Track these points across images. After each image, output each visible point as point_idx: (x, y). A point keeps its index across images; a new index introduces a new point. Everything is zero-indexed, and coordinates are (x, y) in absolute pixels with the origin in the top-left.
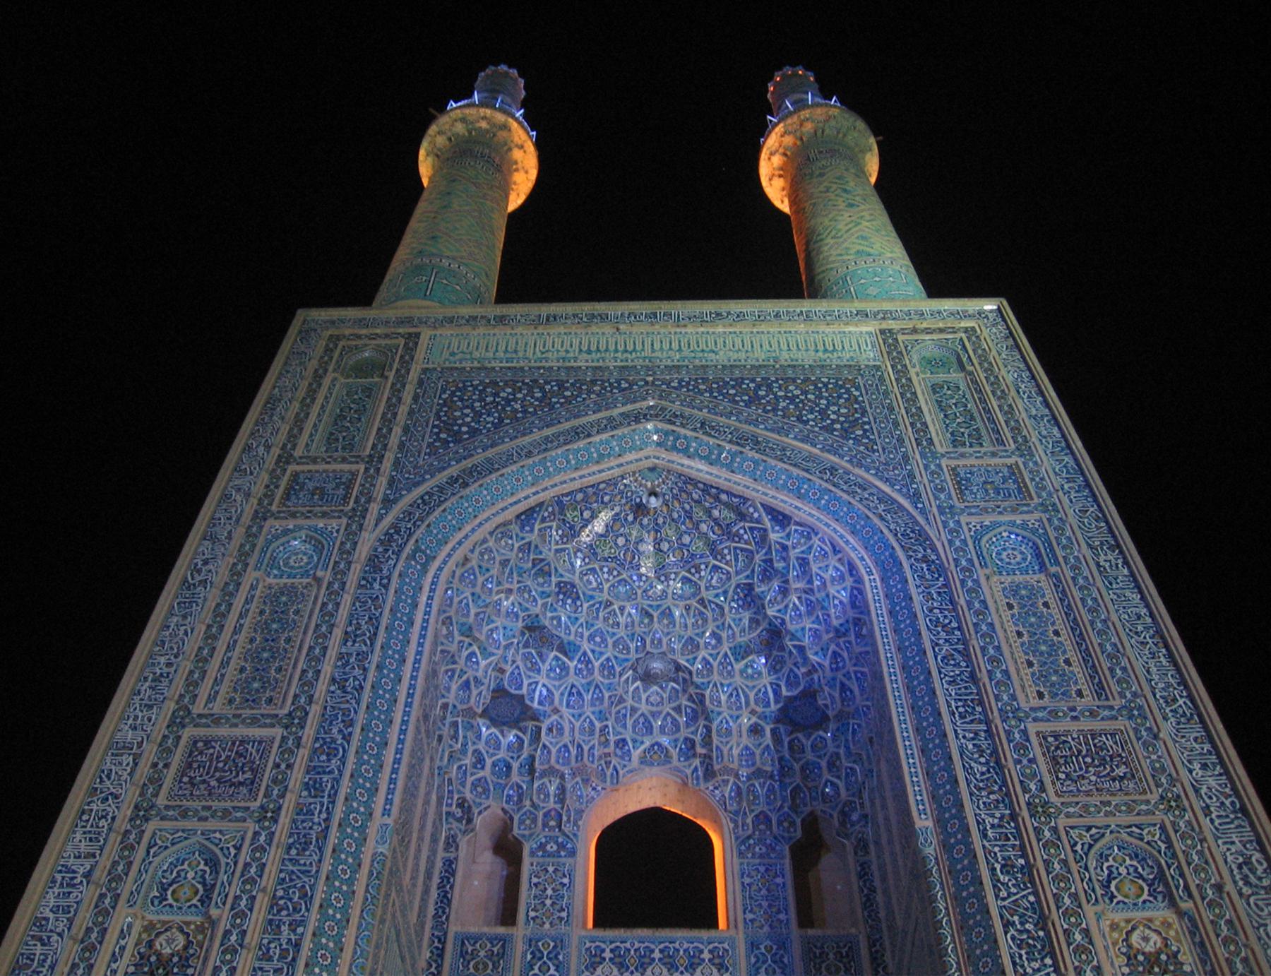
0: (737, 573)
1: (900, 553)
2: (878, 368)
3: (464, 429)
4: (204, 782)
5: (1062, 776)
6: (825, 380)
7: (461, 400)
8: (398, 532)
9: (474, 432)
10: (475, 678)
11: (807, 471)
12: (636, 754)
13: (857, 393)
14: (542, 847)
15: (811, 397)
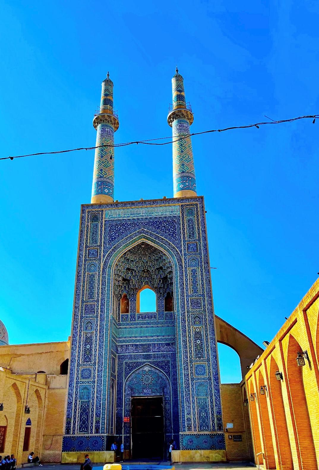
0: (157, 257)
1: (177, 263)
2: (179, 216)
3: (113, 237)
4: (88, 312)
5: (192, 306)
6: (170, 221)
7: (112, 229)
8: (106, 262)
9: (115, 238)
10: (120, 280)
11: (165, 245)
12: (144, 283)
13: (175, 224)
14: (131, 299)
15: (168, 226)
